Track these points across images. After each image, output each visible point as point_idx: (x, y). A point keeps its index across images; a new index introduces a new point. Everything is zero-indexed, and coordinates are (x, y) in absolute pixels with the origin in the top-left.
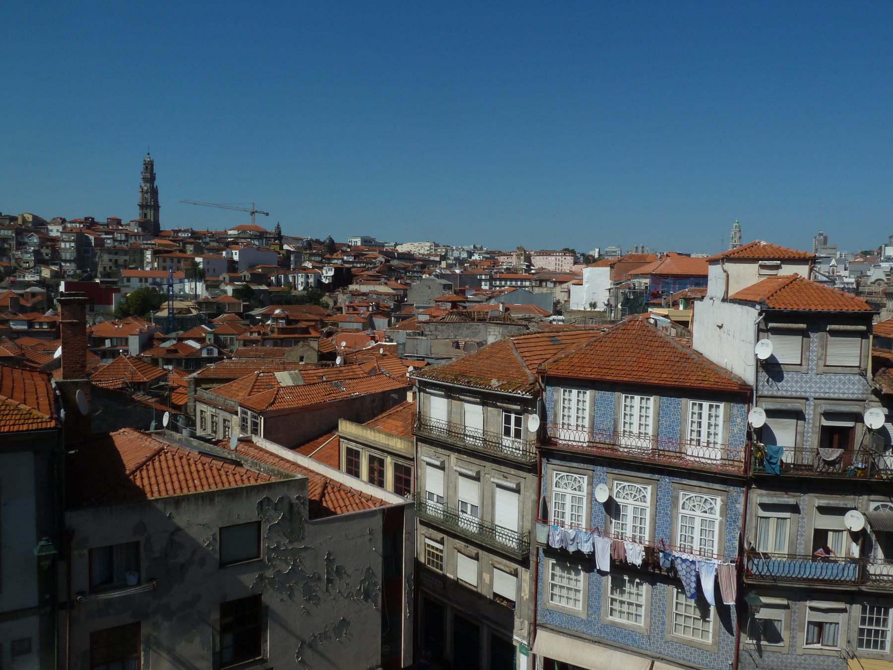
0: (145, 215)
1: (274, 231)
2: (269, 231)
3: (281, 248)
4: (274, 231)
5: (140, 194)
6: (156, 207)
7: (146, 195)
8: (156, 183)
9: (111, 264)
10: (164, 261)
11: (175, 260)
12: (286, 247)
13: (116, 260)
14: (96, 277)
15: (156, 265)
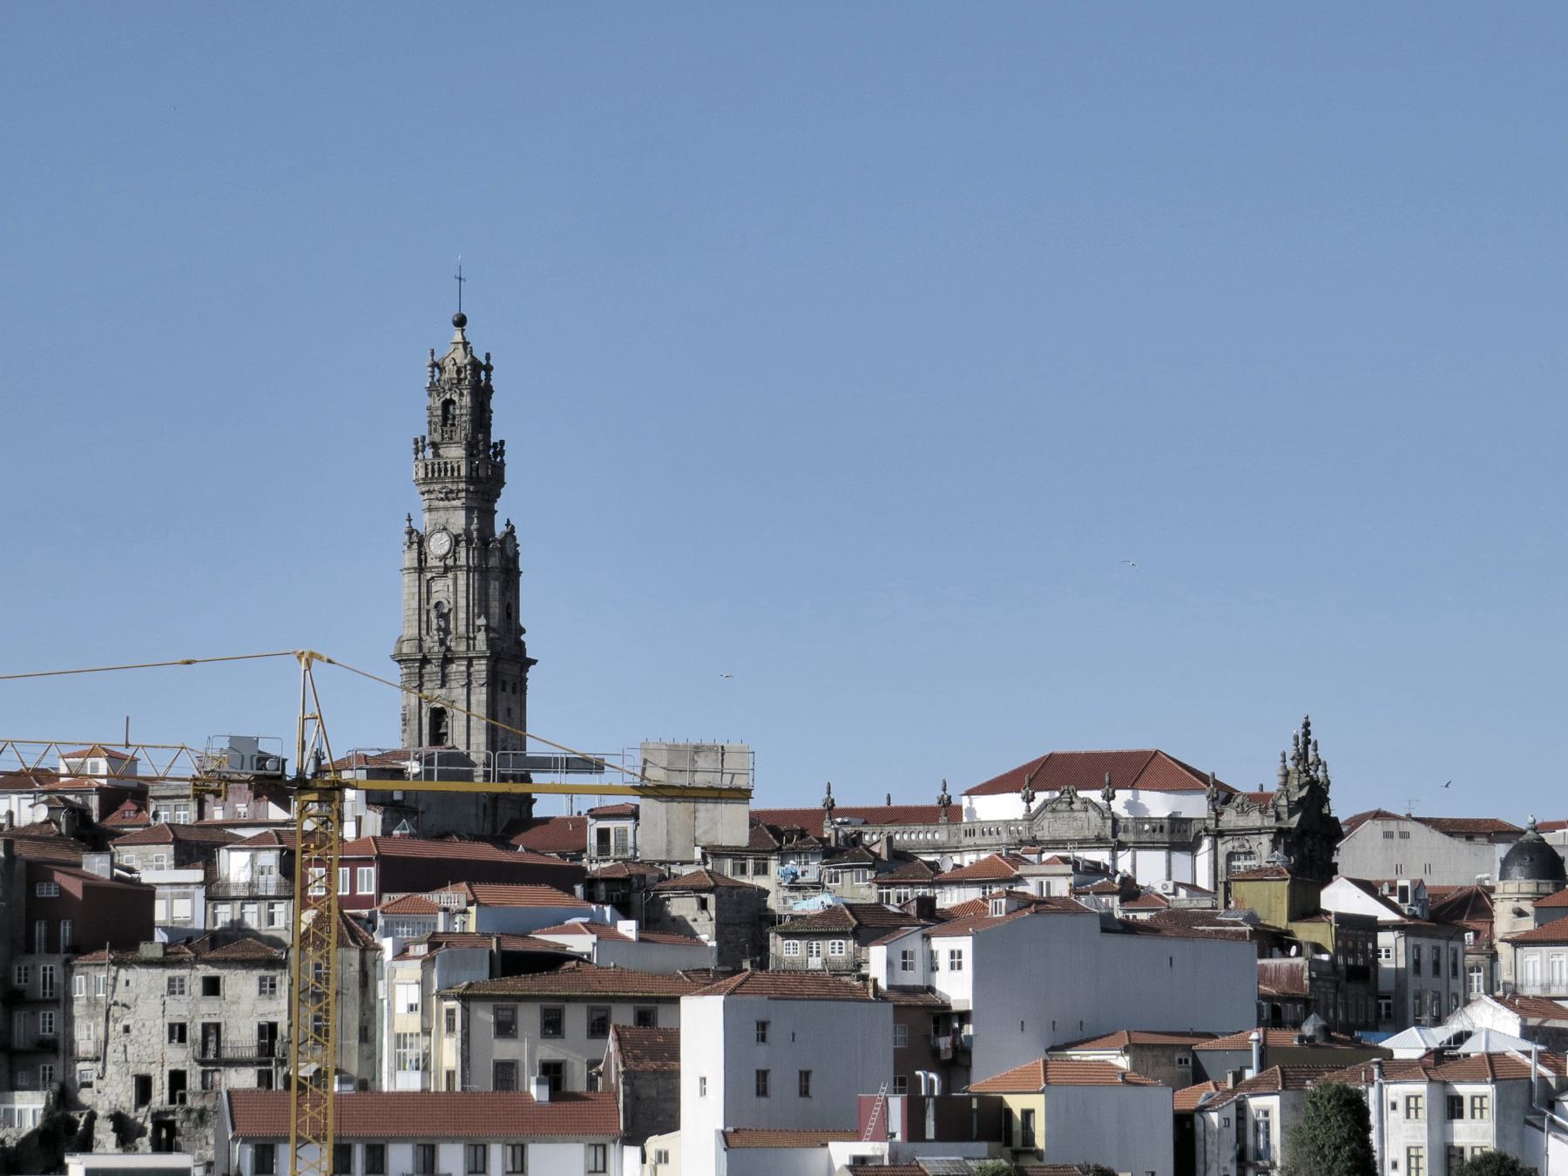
0: (438, 716)
1: (1273, 785)
2: (1245, 784)
3: (1306, 908)
4: (1273, 785)
5: (409, 583)
6: (508, 668)
7: (441, 590)
8: (506, 509)
9: (179, 1057)
10: (505, 1029)
11: (576, 1019)
12: (1340, 897)
13: (212, 1031)
14: (85, 1144)
15: (449, 1054)
